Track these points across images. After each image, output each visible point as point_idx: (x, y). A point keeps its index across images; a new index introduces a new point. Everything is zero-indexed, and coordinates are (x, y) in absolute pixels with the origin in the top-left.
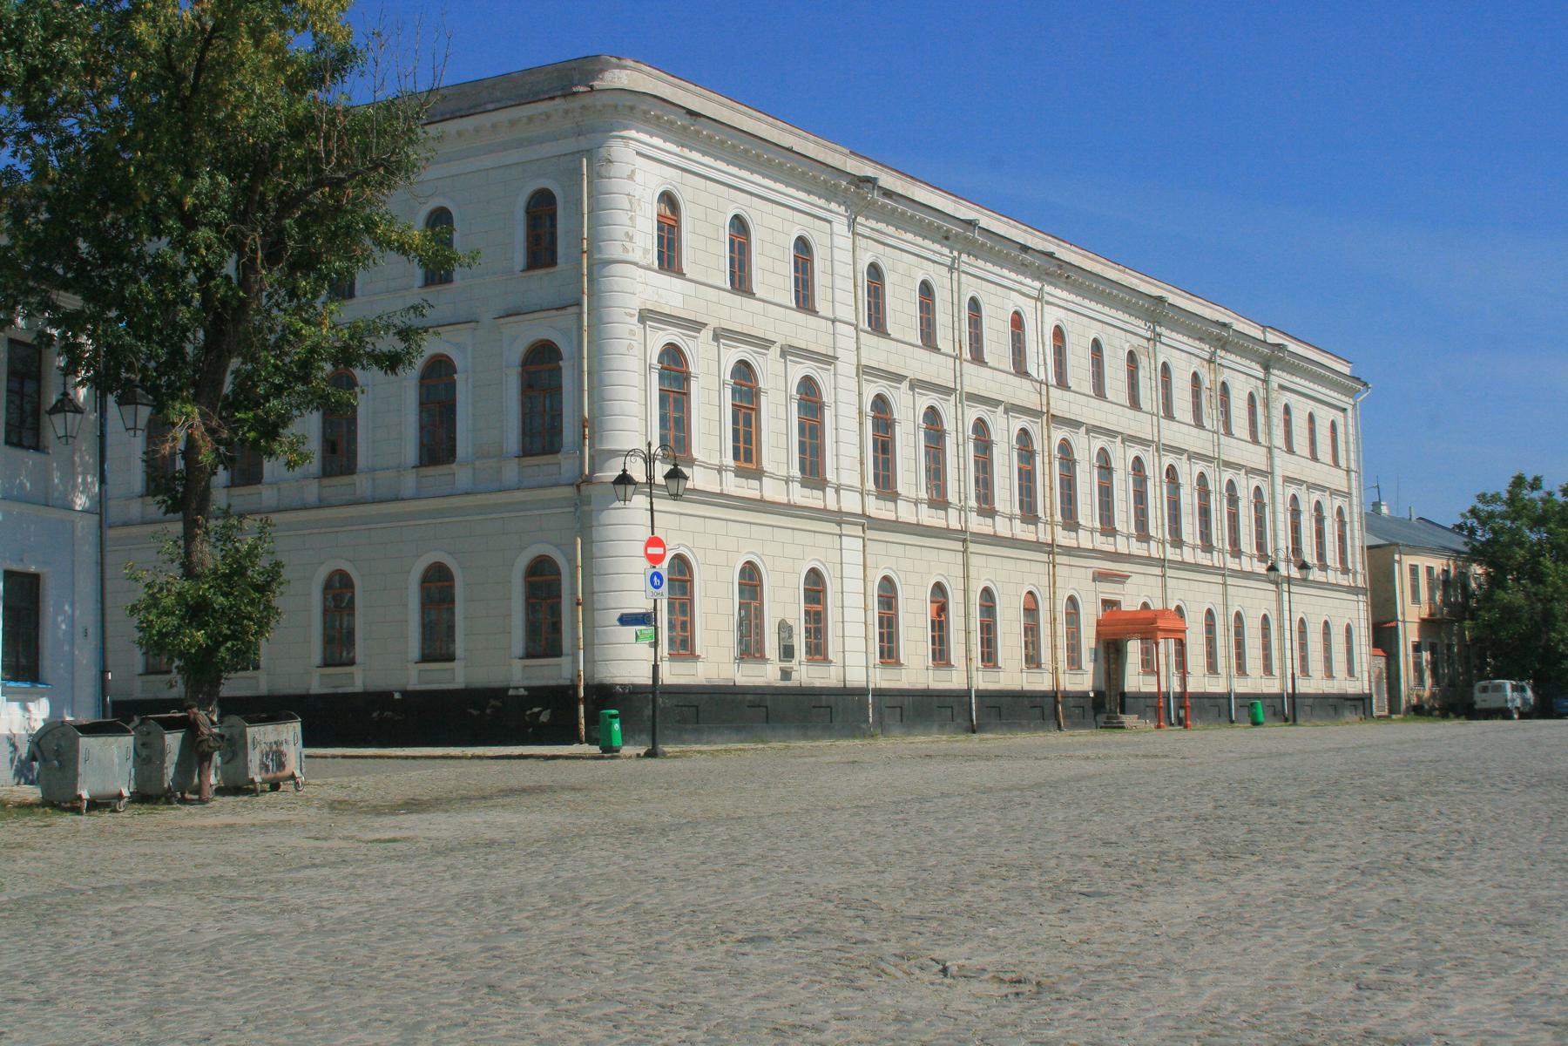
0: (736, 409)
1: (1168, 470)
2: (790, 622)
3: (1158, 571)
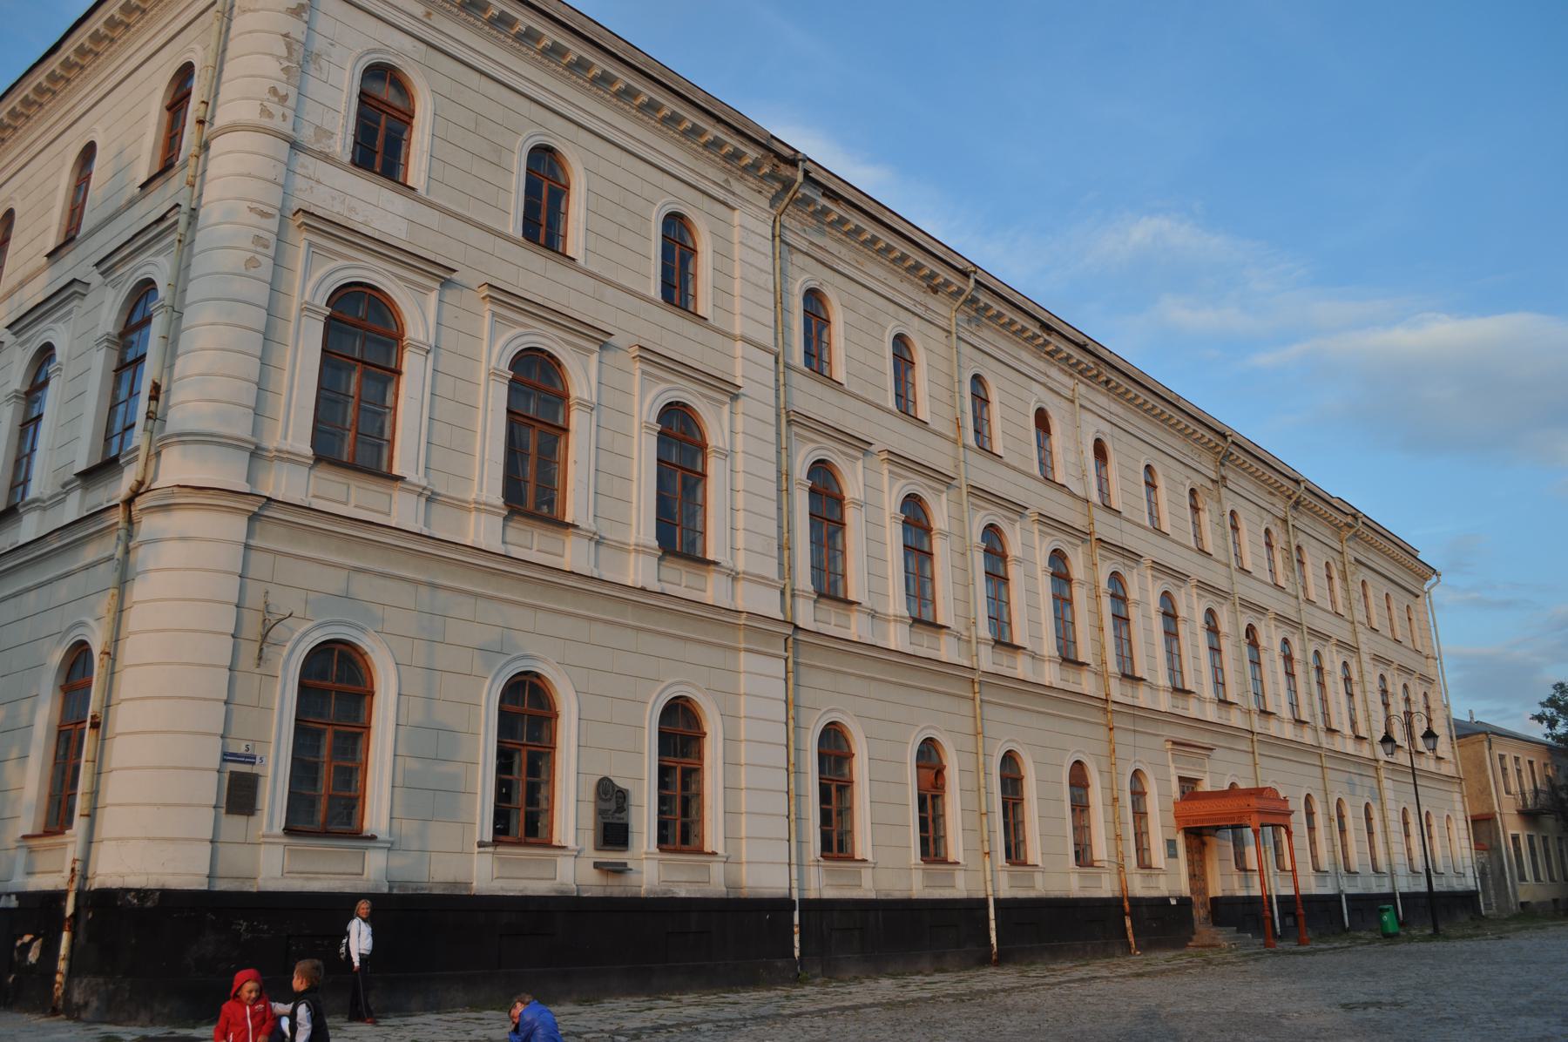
0: (515, 418)
1: (1247, 630)
2: (620, 783)
3: (1245, 746)
